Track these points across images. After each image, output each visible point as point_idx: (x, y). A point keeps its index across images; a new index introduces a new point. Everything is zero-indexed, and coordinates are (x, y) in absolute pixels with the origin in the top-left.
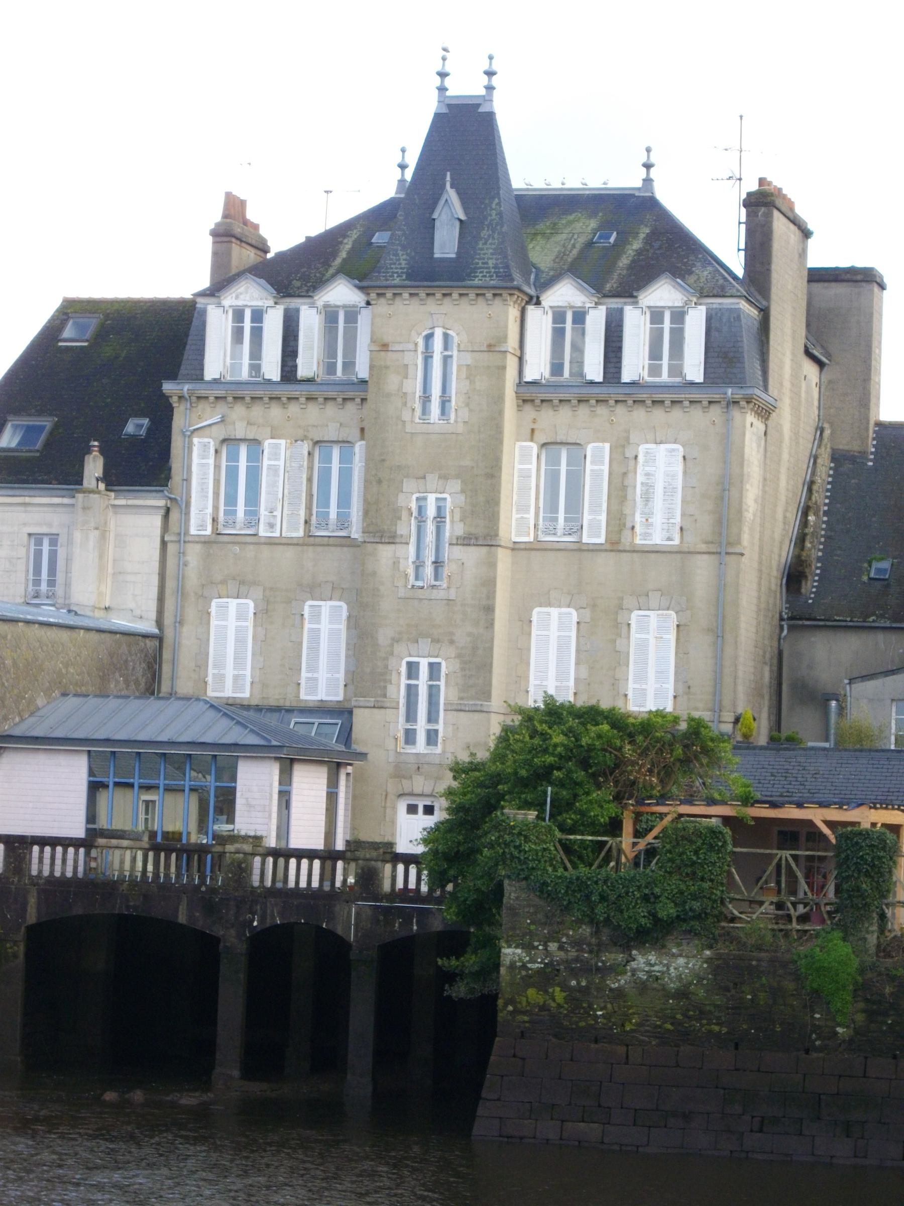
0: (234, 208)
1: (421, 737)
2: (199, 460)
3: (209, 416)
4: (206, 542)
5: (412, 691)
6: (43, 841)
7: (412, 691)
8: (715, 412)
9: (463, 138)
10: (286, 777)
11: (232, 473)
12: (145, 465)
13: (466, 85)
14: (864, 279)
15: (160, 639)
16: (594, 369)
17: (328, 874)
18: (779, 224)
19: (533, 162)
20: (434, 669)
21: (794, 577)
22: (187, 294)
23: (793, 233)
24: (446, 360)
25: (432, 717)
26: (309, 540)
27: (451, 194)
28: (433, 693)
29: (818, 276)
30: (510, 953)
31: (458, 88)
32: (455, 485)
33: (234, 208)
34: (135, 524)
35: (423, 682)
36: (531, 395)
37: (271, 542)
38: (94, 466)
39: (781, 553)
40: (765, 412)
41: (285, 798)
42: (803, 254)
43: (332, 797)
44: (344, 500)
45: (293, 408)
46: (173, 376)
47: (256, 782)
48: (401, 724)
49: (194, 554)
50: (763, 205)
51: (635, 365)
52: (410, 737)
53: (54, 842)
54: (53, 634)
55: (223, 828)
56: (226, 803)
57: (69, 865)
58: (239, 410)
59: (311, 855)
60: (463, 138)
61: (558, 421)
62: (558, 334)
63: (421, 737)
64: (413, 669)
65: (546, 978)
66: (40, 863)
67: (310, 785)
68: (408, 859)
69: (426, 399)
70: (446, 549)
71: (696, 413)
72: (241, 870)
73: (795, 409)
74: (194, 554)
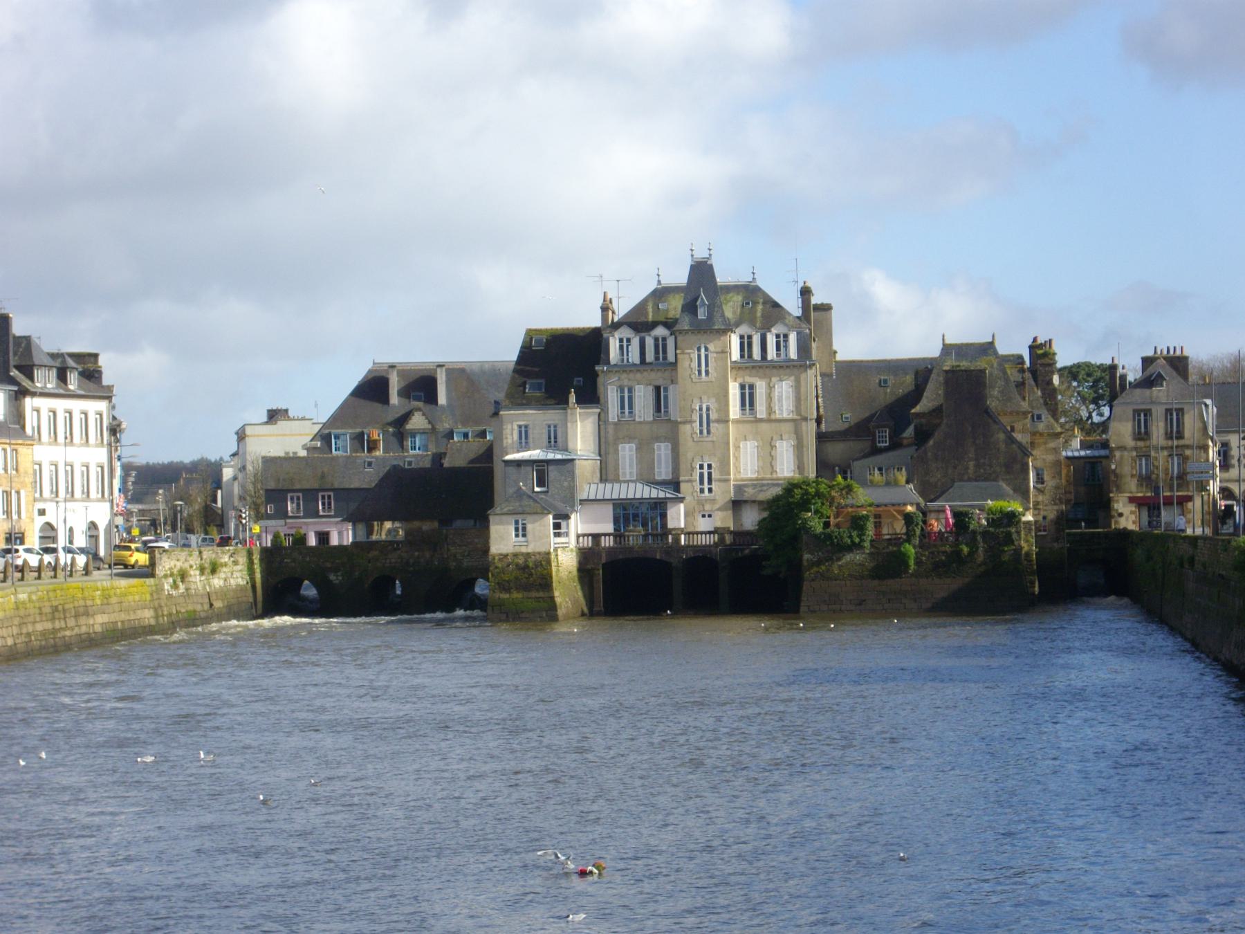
2: (612, 396)
4: (615, 424)
5: (702, 475)
7: (702, 475)
9: (702, 271)
13: (701, 254)
19: (723, 276)
24: (706, 356)
28: (710, 474)
32: (713, 400)
35: (705, 471)
37: (640, 423)
38: (572, 398)
46: (598, 364)
49: (611, 429)
50: (806, 292)
51: (772, 353)
52: (702, 491)
58: (624, 376)
60: (702, 271)
62: (742, 344)
64: (701, 467)
69: (700, 372)
72: (677, 540)
74: (611, 429)
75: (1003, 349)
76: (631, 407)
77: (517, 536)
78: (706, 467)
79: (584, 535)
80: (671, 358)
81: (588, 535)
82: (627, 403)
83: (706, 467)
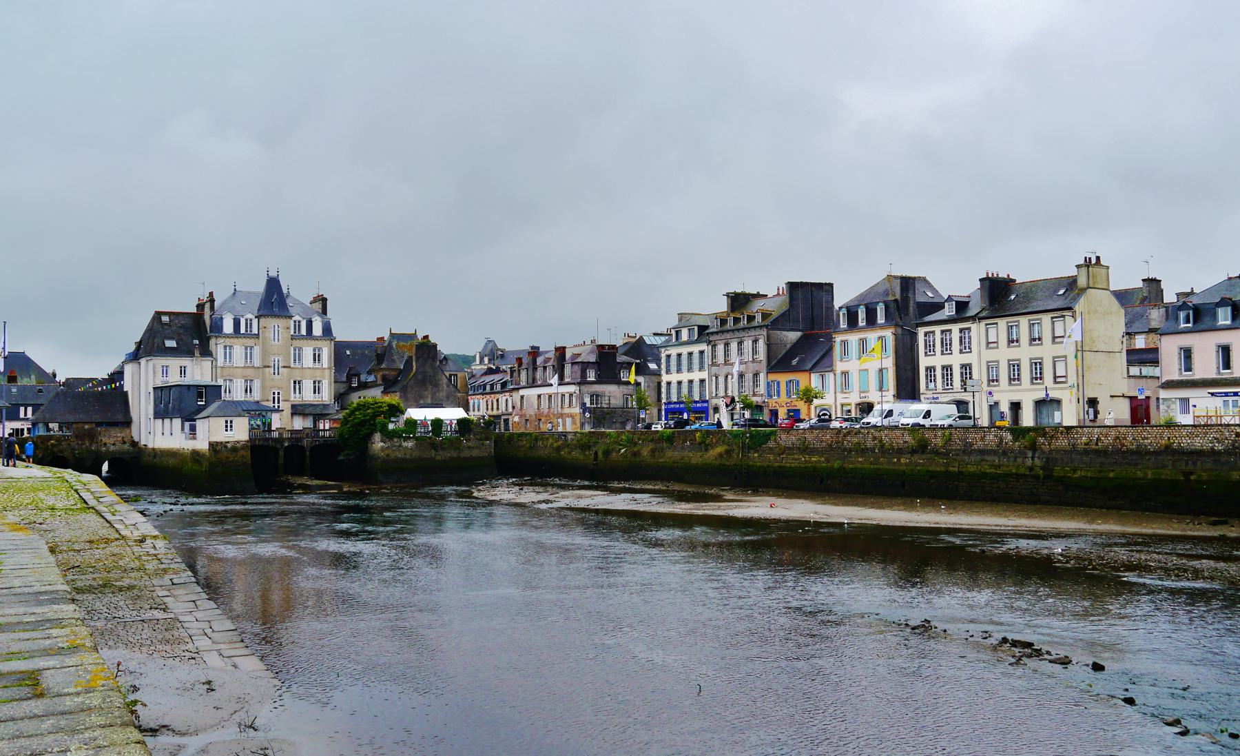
3: (221, 341)
9: (273, 285)
12: (206, 352)
13: (273, 274)
16: (304, 332)
34: (207, 363)
49: (219, 371)
60: (273, 285)
61: (298, 343)
80: (255, 331)
82: (228, 355)
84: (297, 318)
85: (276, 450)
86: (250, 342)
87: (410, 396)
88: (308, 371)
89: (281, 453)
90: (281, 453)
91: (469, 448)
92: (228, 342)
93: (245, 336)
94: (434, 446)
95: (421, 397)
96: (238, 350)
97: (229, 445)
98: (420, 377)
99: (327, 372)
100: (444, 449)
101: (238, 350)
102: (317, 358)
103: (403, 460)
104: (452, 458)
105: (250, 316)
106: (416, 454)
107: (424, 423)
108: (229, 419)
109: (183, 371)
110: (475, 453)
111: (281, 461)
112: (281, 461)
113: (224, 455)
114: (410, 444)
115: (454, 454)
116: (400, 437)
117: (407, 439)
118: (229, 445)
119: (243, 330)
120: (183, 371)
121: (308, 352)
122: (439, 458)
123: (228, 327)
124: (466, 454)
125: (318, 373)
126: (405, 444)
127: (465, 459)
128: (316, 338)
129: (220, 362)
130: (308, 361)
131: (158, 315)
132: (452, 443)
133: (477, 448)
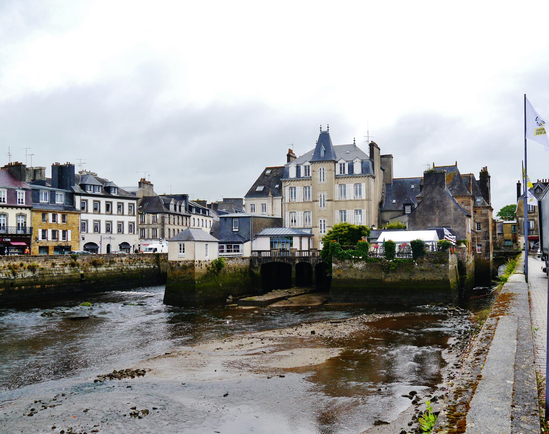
0: (290, 151)
1: (323, 232)
2: (286, 191)
3: (288, 183)
6: (263, 251)
8: (366, 178)
9: (324, 138)
10: (301, 239)
11: (292, 192)
12: (279, 192)
13: (324, 129)
14: (390, 156)
15: (282, 219)
16: (347, 172)
17: (309, 254)
18: (375, 148)
20: (324, 221)
21: (381, 204)
22: (283, 166)
23: (378, 150)
25: (324, 229)
26: (304, 202)
27: (323, 147)
28: (324, 225)
29: (382, 156)
30: (333, 265)
31: (323, 130)
32: (326, 192)
33: (290, 151)
34: (278, 202)
35: (323, 223)
36: (337, 177)
37: (298, 203)
39: (378, 200)
40: (374, 178)
41: (301, 242)
42: (379, 153)
43: (309, 242)
44: (309, 196)
45: (301, 182)
47: (296, 240)
48: (320, 230)
49: (287, 205)
50: (372, 146)
52: (321, 232)
53: (265, 251)
54: (264, 219)
55: (291, 248)
56: (291, 245)
57: (268, 254)
59: (306, 251)
60: (324, 138)
61: (341, 181)
63: (323, 232)
64: (321, 221)
65: (339, 269)
66: (263, 254)
67: (305, 241)
68: (319, 251)
70: (325, 202)
71: (363, 178)
72: (294, 254)
73: (379, 177)
74: (287, 205)
75: (463, 171)
76: (295, 196)
77: (181, 252)
78: (323, 221)
79: (254, 251)
80: (311, 175)
81: (256, 251)
82: (293, 194)
83: (323, 221)
84: (342, 161)
85: (290, 266)
86: (307, 183)
87: (418, 220)
88: (350, 203)
89: (294, 269)
90: (294, 269)
91: (422, 270)
92: (293, 184)
93: (304, 179)
94: (387, 269)
95: (429, 220)
96: (299, 190)
97: (181, 264)
98: (428, 202)
99: (365, 203)
100: (394, 271)
101: (299, 190)
102: (358, 192)
103: (353, 281)
104: (402, 281)
105: (307, 164)
106: (366, 275)
107: (404, 244)
108: (182, 243)
109: (264, 207)
110: (428, 276)
111: (293, 275)
112: (293, 275)
113: (178, 271)
114: (360, 266)
115: (405, 276)
116: (350, 258)
117: (357, 260)
118: (181, 264)
119: (302, 174)
120: (264, 207)
121: (350, 187)
122: (388, 280)
123: (292, 174)
124: (419, 276)
125: (358, 204)
126: (355, 265)
127: (418, 282)
128: (357, 176)
129: (287, 200)
130: (350, 193)
131: (267, 169)
132: (401, 265)
133: (431, 271)
